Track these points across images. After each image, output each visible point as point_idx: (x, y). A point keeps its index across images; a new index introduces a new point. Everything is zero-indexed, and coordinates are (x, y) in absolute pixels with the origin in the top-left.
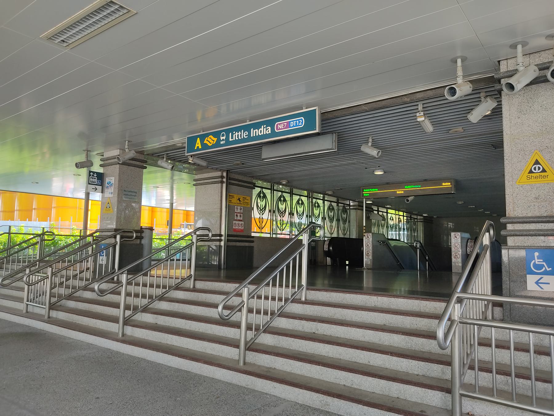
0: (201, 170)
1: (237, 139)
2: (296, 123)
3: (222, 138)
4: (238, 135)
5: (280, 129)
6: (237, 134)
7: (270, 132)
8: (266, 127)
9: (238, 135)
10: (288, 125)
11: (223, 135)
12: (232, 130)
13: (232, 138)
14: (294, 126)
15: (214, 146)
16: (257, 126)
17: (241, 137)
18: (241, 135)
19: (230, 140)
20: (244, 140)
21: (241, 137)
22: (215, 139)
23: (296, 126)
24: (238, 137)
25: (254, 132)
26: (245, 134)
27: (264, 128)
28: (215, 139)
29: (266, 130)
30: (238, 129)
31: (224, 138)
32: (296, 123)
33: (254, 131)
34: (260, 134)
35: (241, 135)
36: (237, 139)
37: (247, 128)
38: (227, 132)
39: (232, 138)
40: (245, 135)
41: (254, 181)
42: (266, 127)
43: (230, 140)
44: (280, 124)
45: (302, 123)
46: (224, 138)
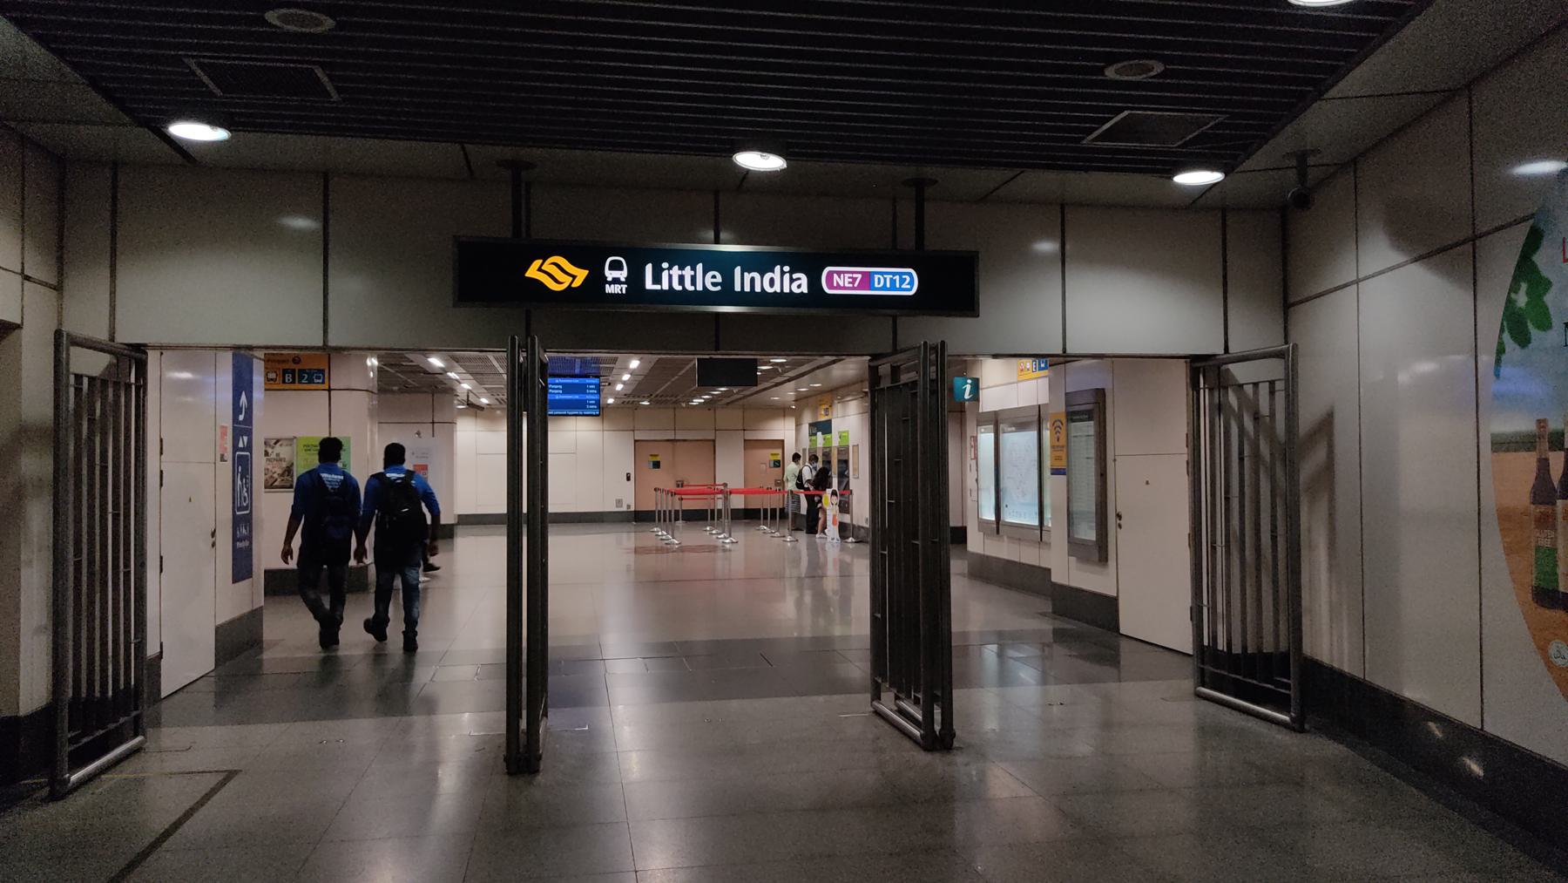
0: (406, 389)
1: (677, 287)
3: (610, 275)
4: (681, 278)
5: (838, 287)
8: (791, 273)
9: (681, 278)
11: (616, 266)
13: (657, 279)
14: (884, 288)
17: (693, 282)
21: (693, 282)
22: (582, 274)
23: (893, 288)
27: (783, 273)
28: (582, 274)
29: (792, 280)
31: (622, 275)
32: (902, 281)
33: (748, 276)
34: (769, 290)
42: (791, 273)
43: (649, 285)
44: (839, 273)
45: (911, 283)
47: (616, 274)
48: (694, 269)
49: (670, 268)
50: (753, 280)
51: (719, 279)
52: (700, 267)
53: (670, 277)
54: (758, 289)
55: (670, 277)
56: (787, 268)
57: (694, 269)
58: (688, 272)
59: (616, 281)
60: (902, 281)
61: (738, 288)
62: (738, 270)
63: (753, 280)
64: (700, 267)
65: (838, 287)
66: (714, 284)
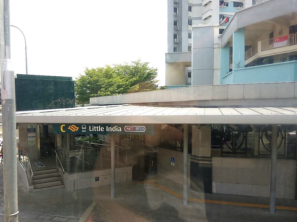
1: (95, 130)
2: (140, 129)
3: (83, 128)
4: (96, 128)
6: (95, 127)
7: (121, 131)
9: (96, 128)
11: (84, 127)
13: (91, 129)
14: (138, 130)
18: (98, 129)
19: (90, 130)
24: (96, 130)
27: (116, 127)
29: (118, 129)
35: (98, 129)
36: (95, 130)
37: (104, 125)
39: (91, 129)
43: (90, 130)
45: (144, 129)
47: (84, 128)
49: (94, 127)
50: (110, 129)
51: (103, 129)
52: (99, 126)
53: (94, 128)
54: (111, 131)
55: (94, 128)
56: (117, 126)
61: (107, 131)
62: (107, 127)
63: (110, 129)
64: (99, 126)
66: (102, 130)
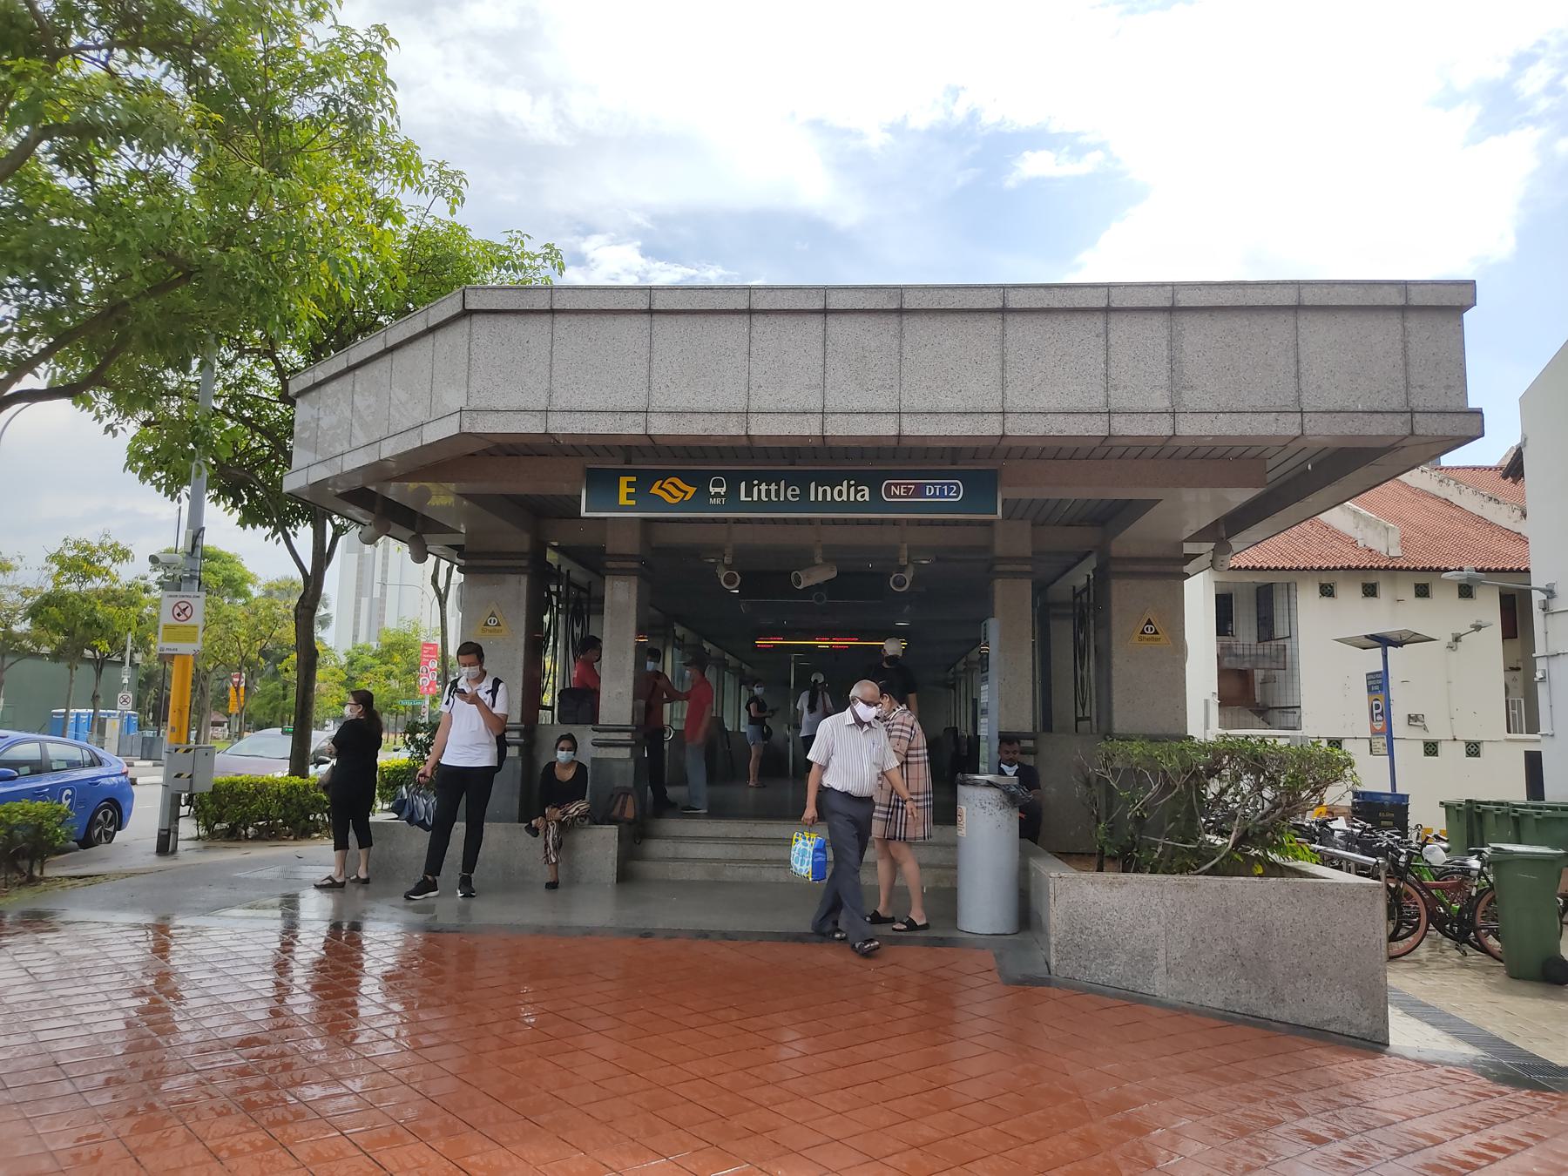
2: (942, 490)
3: (713, 490)
5: (895, 496)
6: (763, 487)
9: (768, 492)
10: (919, 491)
11: (718, 484)
12: (749, 477)
13: (749, 493)
14: (934, 496)
15: (683, 506)
16: (833, 480)
17: (778, 495)
18: (778, 491)
20: (786, 506)
21: (778, 495)
22: (692, 490)
25: (816, 493)
26: (789, 492)
27: (849, 487)
29: (857, 492)
30: (768, 478)
31: (722, 490)
32: (950, 490)
33: (820, 490)
35: (778, 491)
38: (733, 480)
40: (792, 493)
41: (1177, 568)
42: (856, 486)
43: (743, 498)
44: (896, 485)
45: (958, 492)
46: (722, 490)
48: (778, 485)
57: (778, 485)
58: (773, 487)
59: (718, 495)
60: (950, 490)
65: (895, 496)
